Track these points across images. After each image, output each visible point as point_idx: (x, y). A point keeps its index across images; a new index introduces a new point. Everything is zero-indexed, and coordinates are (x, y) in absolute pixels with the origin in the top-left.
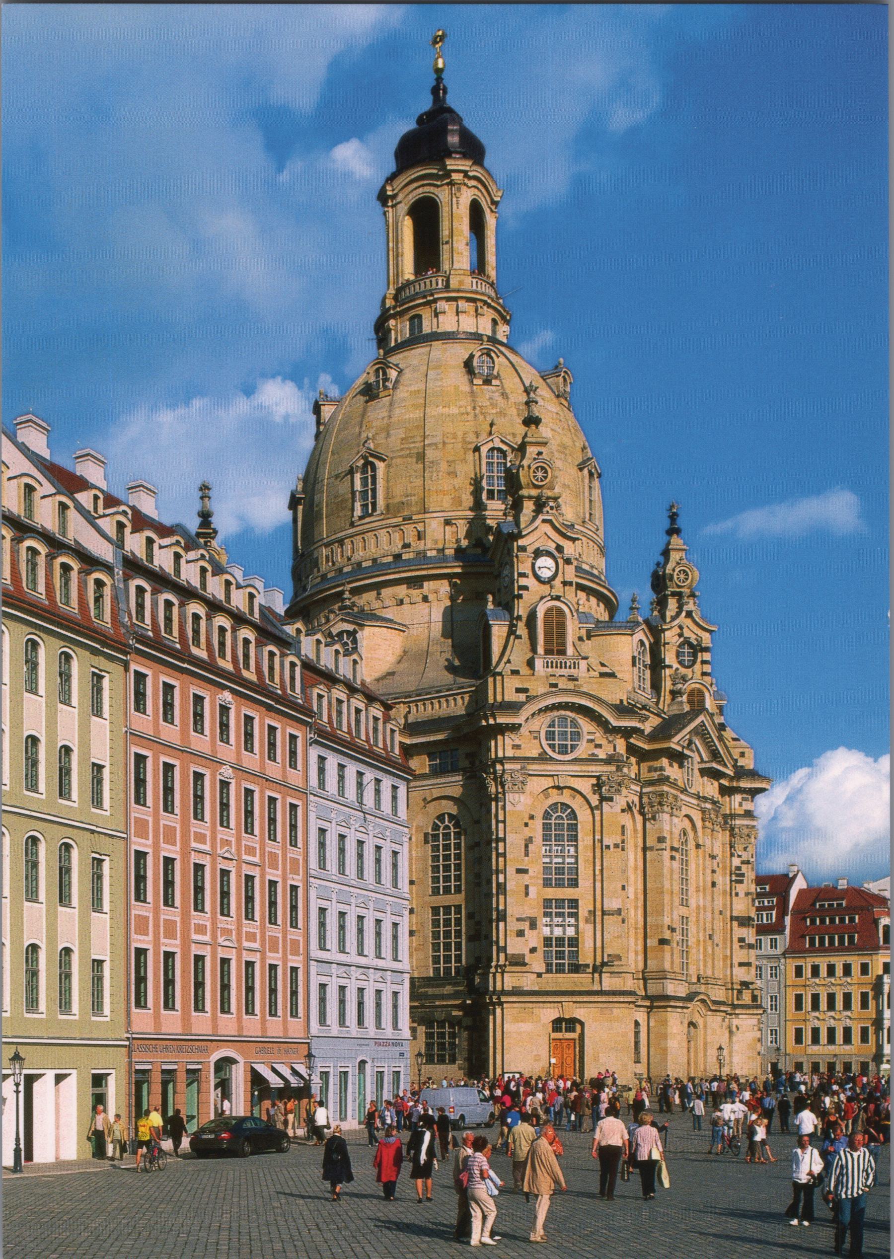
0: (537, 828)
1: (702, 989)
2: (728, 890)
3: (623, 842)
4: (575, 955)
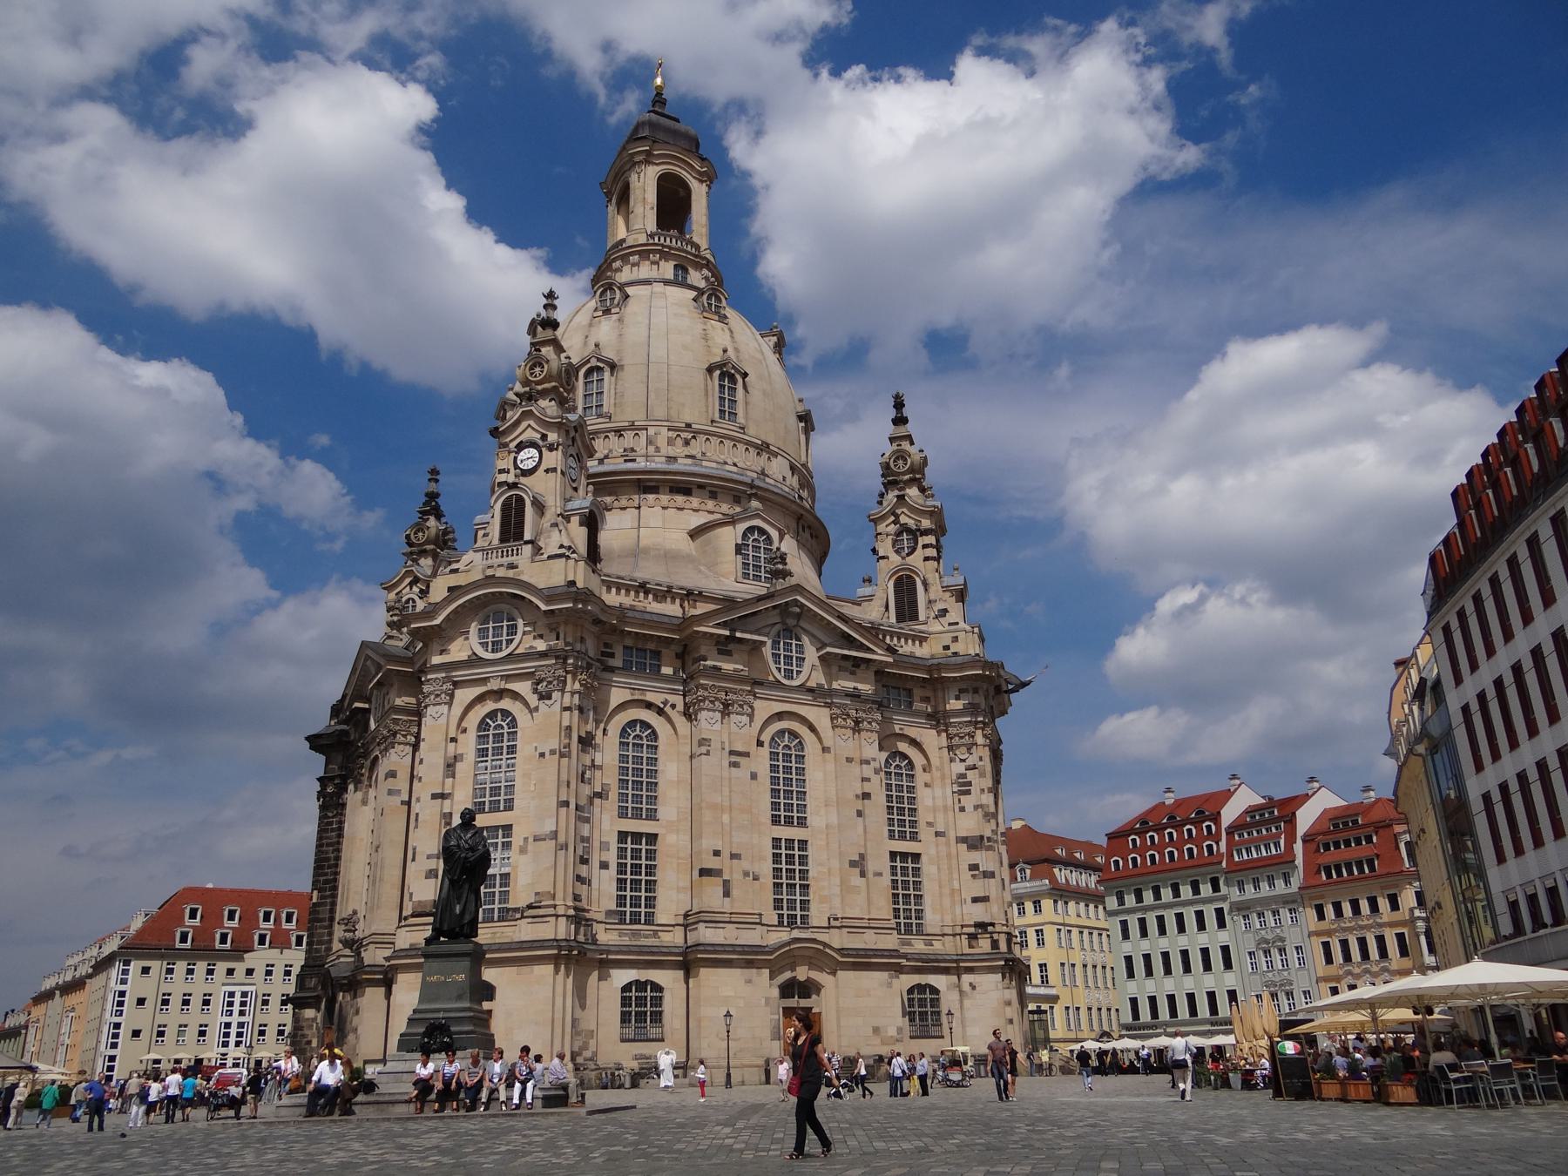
0: (468, 745)
4: (505, 896)
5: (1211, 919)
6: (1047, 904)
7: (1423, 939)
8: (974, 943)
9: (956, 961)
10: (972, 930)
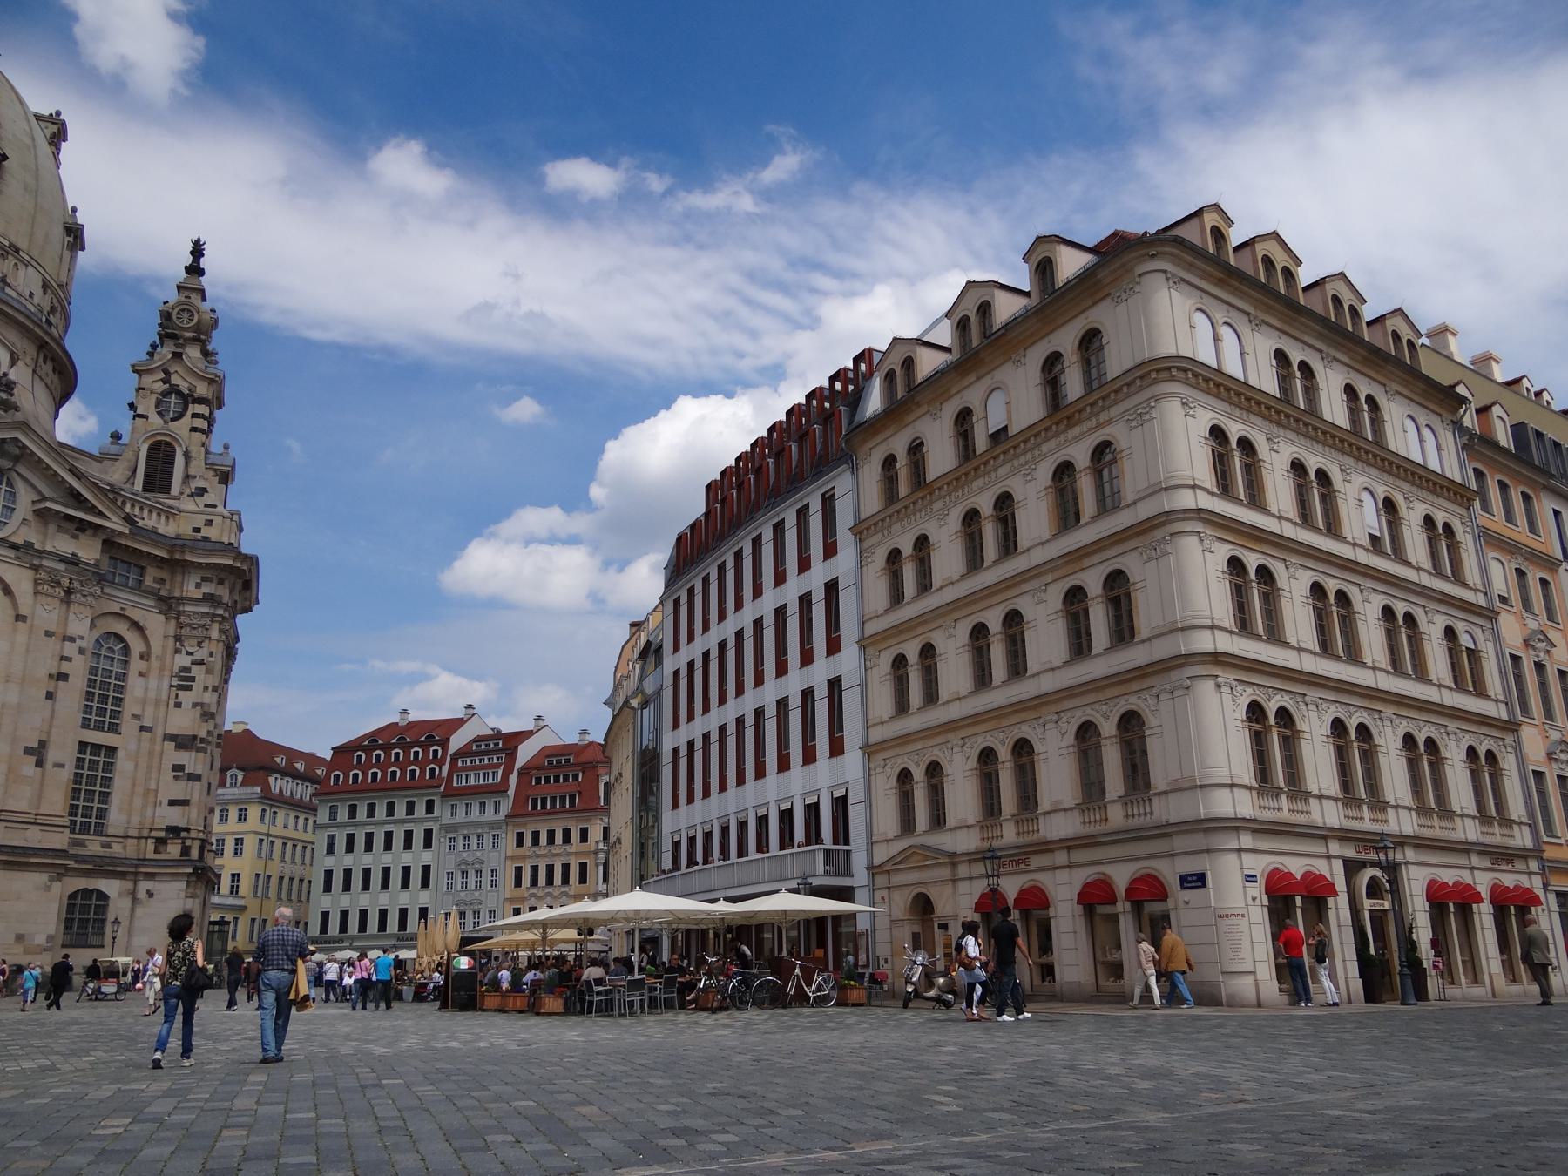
2: (164, 696)
5: (418, 840)
6: (254, 812)
7: (601, 868)
8: (161, 848)
9: (137, 866)
10: (162, 834)
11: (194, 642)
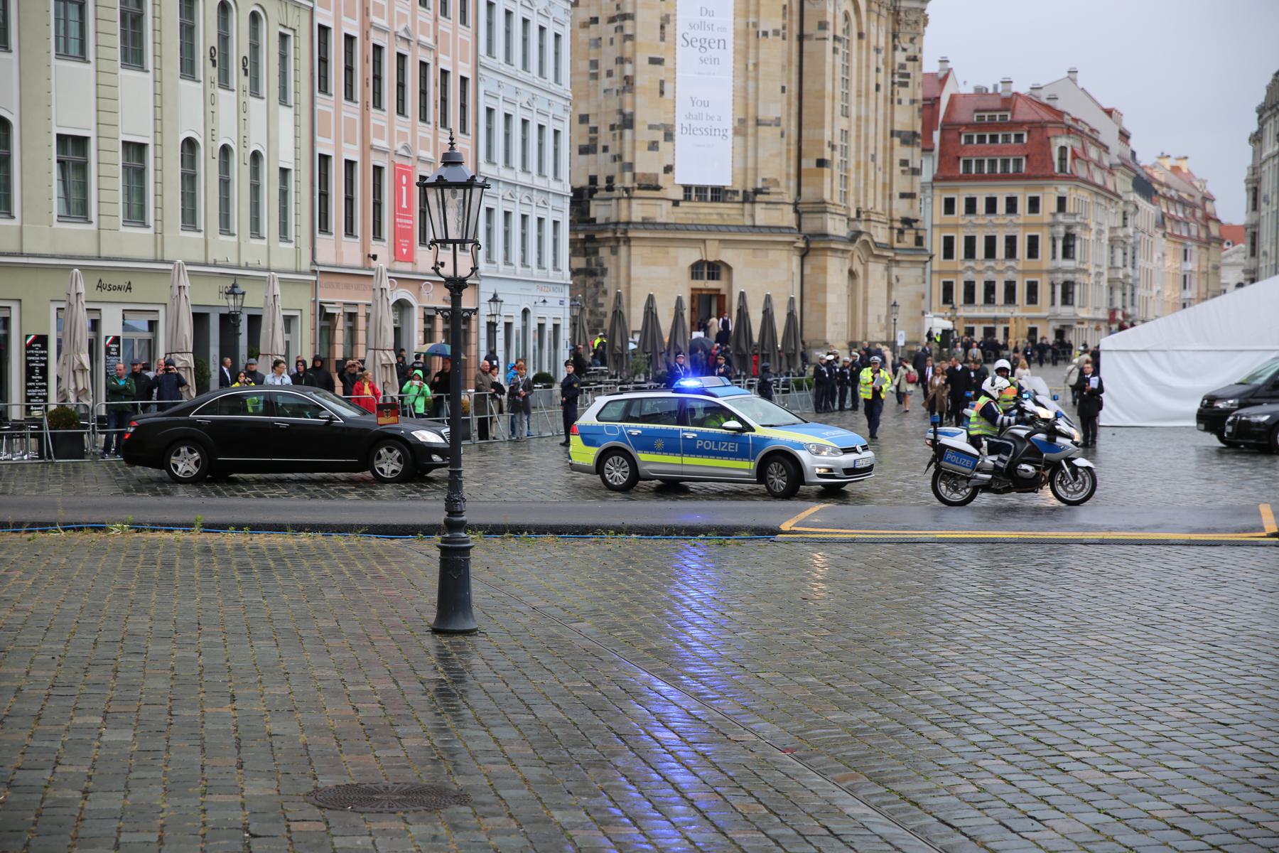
1: (862, 227)
3: (784, 28)
11: (907, 39)
